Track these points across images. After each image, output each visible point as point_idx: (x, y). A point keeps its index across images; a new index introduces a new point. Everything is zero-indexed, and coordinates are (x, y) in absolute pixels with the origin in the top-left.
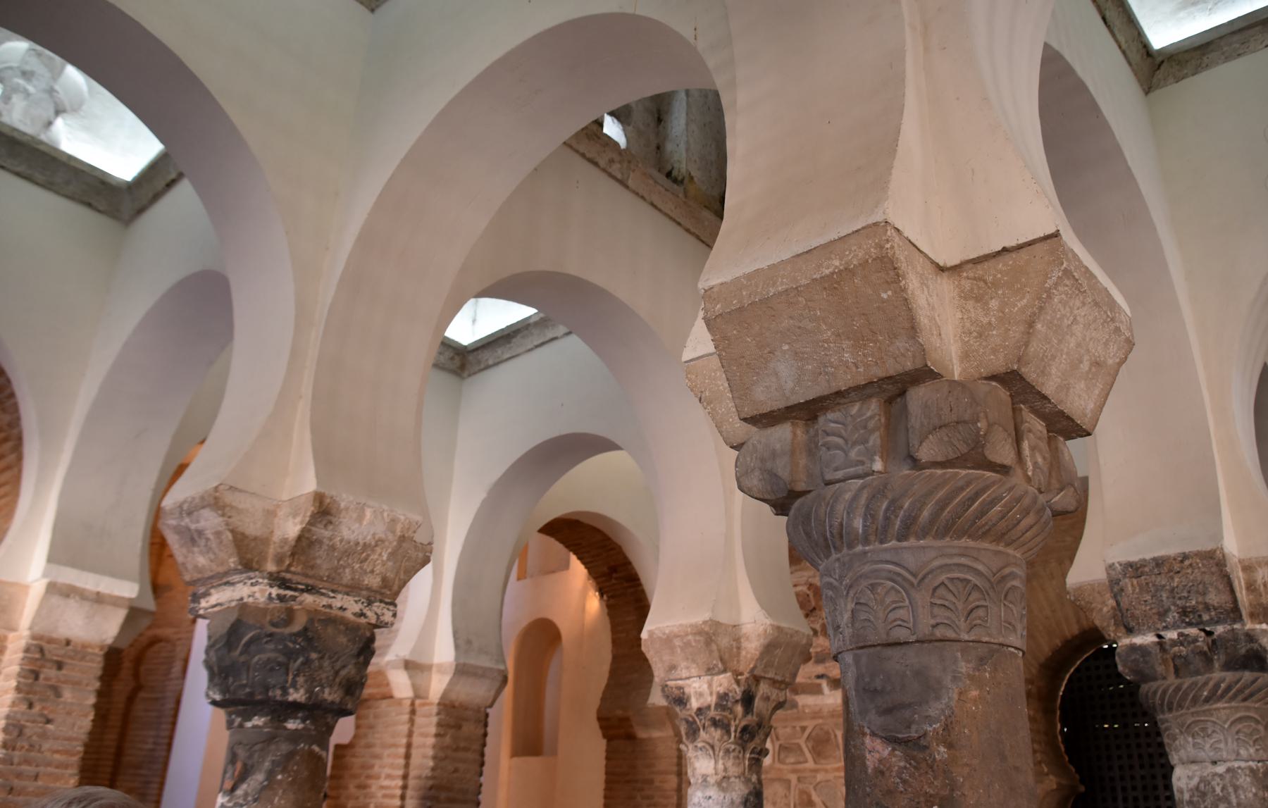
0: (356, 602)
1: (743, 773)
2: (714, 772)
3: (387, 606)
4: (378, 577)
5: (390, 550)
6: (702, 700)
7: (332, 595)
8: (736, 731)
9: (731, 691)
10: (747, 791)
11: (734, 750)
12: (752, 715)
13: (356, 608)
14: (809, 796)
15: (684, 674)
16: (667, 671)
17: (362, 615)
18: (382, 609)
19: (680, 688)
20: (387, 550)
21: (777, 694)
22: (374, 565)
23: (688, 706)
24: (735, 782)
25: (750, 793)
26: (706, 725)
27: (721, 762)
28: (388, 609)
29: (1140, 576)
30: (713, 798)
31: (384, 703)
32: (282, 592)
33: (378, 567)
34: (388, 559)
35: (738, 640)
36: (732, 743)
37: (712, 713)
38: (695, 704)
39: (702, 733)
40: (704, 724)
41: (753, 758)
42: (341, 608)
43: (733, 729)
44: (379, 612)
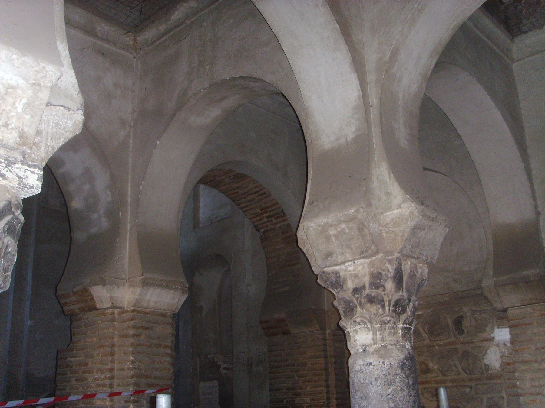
1: (398, 342)
2: (372, 342)
3: (32, 169)
4: (14, 132)
5: (24, 101)
6: (357, 281)
8: (389, 306)
9: (384, 270)
10: (403, 356)
11: (389, 322)
14: (427, 365)
15: (340, 259)
16: (324, 259)
18: (25, 172)
19: (337, 273)
20: (21, 101)
23: (345, 288)
24: (392, 349)
25: (406, 358)
26: (362, 301)
27: (378, 333)
28: (32, 172)
30: (373, 364)
31: (90, 316)
33: (14, 120)
34: (24, 111)
37: (367, 291)
38: (350, 285)
39: (359, 309)
40: (360, 302)
41: (406, 328)
43: (386, 304)
44: (21, 174)
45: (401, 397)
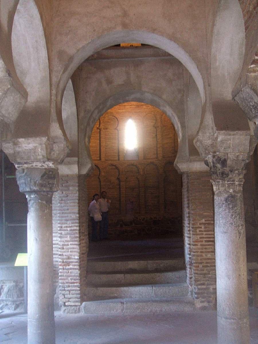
7: (32, 163)
13: (40, 165)
25: (229, 197)
32: (18, 166)
42: (36, 166)
44: (48, 164)
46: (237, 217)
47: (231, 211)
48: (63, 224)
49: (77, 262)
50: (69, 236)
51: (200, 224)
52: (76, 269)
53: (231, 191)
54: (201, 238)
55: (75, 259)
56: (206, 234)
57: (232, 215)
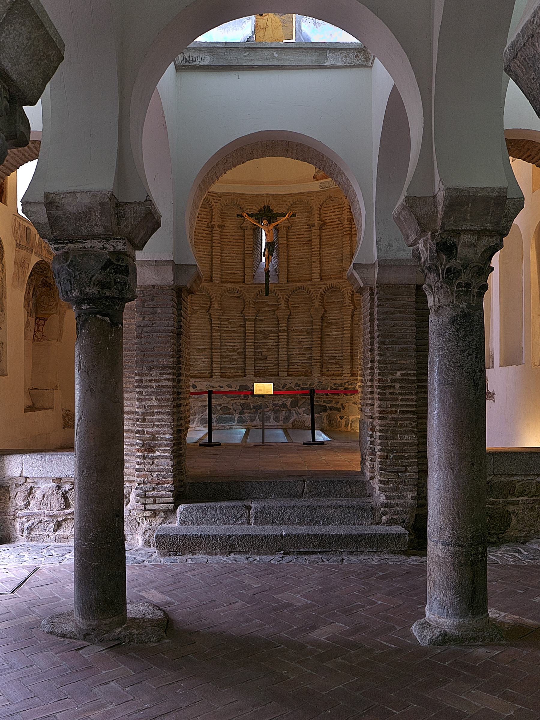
0: (99, 242)
3: (119, 241)
7: (84, 241)
8: (443, 274)
12: (456, 259)
13: (100, 245)
17: (104, 248)
21: (488, 240)
22: (96, 221)
25: (458, 315)
27: (436, 296)
28: (119, 242)
29: (517, 54)
32: (56, 246)
35: (436, 207)
36: (441, 282)
42: (91, 247)
45: (448, 346)
46: (472, 355)
47: (462, 343)
48: (143, 375)
49: (167, 445)
50: (154, 398)
51: (392, 381)
52: (166, 457)
53: (463, 305)
54: (392, 406)
55: (165, 439)
56: (401, 400)
57: (464, 351)
